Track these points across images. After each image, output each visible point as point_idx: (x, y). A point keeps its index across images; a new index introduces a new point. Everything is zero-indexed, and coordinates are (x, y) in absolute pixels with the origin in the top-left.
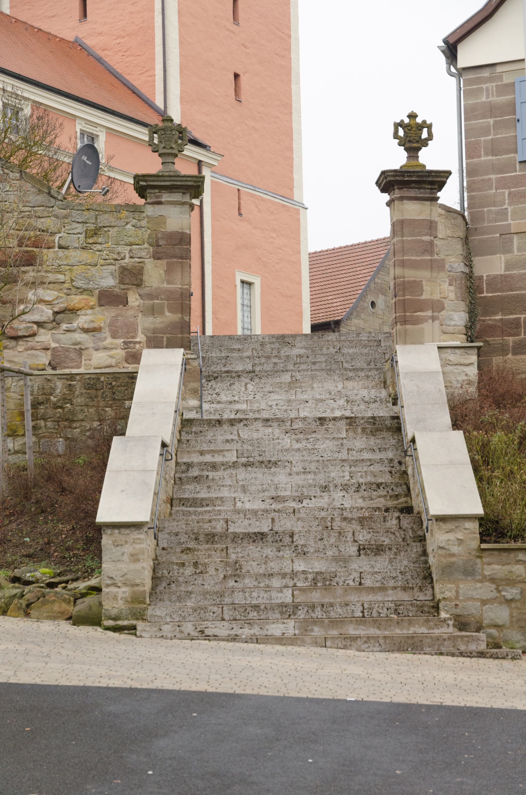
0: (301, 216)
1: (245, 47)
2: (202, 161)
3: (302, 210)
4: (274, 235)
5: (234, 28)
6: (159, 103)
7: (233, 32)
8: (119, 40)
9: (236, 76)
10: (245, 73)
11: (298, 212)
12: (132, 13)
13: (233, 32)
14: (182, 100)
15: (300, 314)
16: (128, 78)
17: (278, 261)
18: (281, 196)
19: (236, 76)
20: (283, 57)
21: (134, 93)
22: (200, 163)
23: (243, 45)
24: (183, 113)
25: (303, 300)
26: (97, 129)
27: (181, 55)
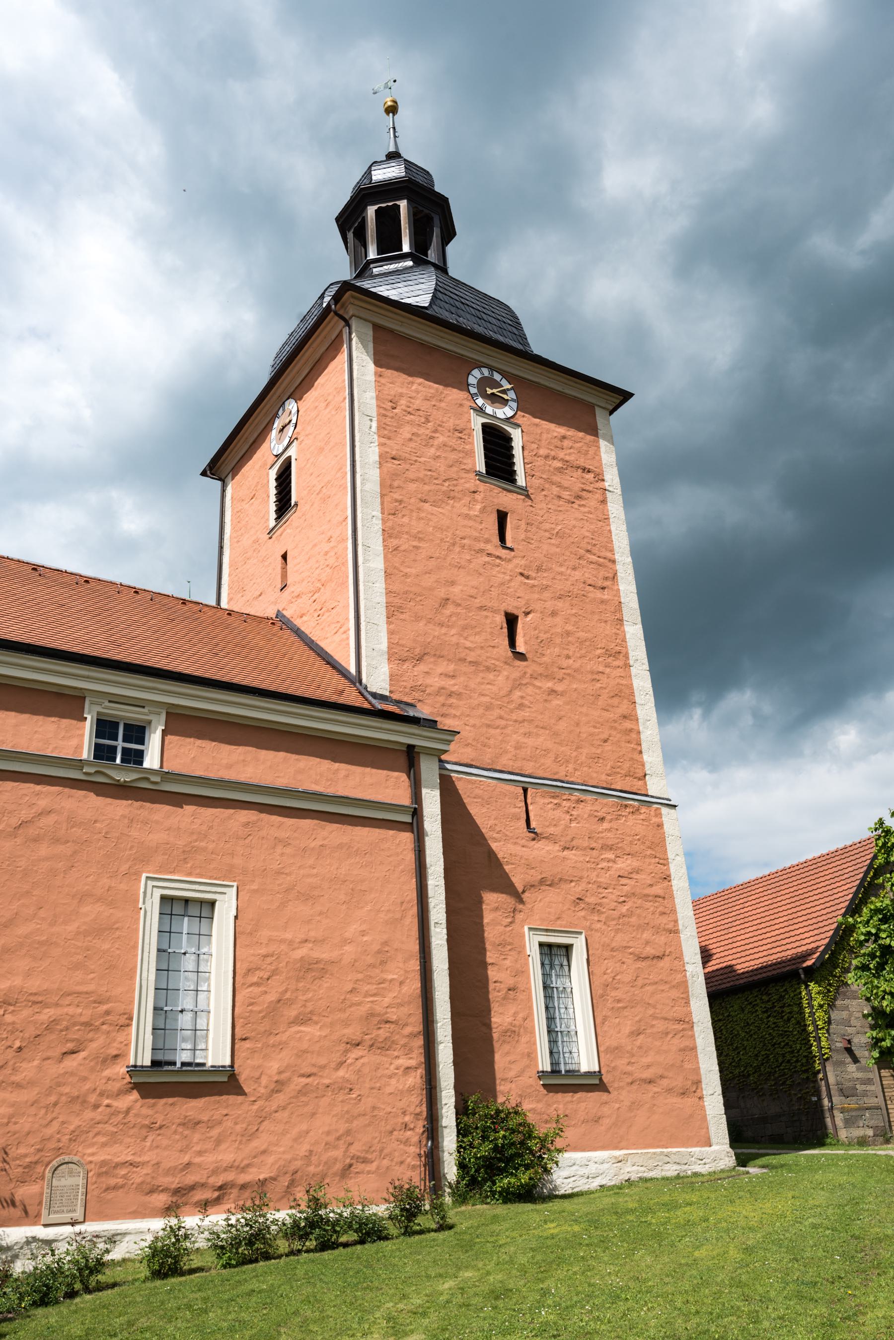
0: (665, 819)
1: (528, 578)
2: (413, 746)
3: (665, 810)
4: (610, 855)
5: (503, 553)
6: (353, 670)
7: (498, 557)
8: (314, 598)
9: (511, 621)
10: (527, 614)
11: (659, 815)
12: (326, 553)
13: (498, 557)
14: (392, 656)
15: (683, 986)
16: (322, 644)
17: (622, 899)
18: (621, 791)
19: (511, 621)
20: (603, 588)
21: (328, 663)
22: (411, 748)
23: (522, 574)
24: (393, 678)
25: (686, 959)
26: (145, 710)
27: (389, 592)
